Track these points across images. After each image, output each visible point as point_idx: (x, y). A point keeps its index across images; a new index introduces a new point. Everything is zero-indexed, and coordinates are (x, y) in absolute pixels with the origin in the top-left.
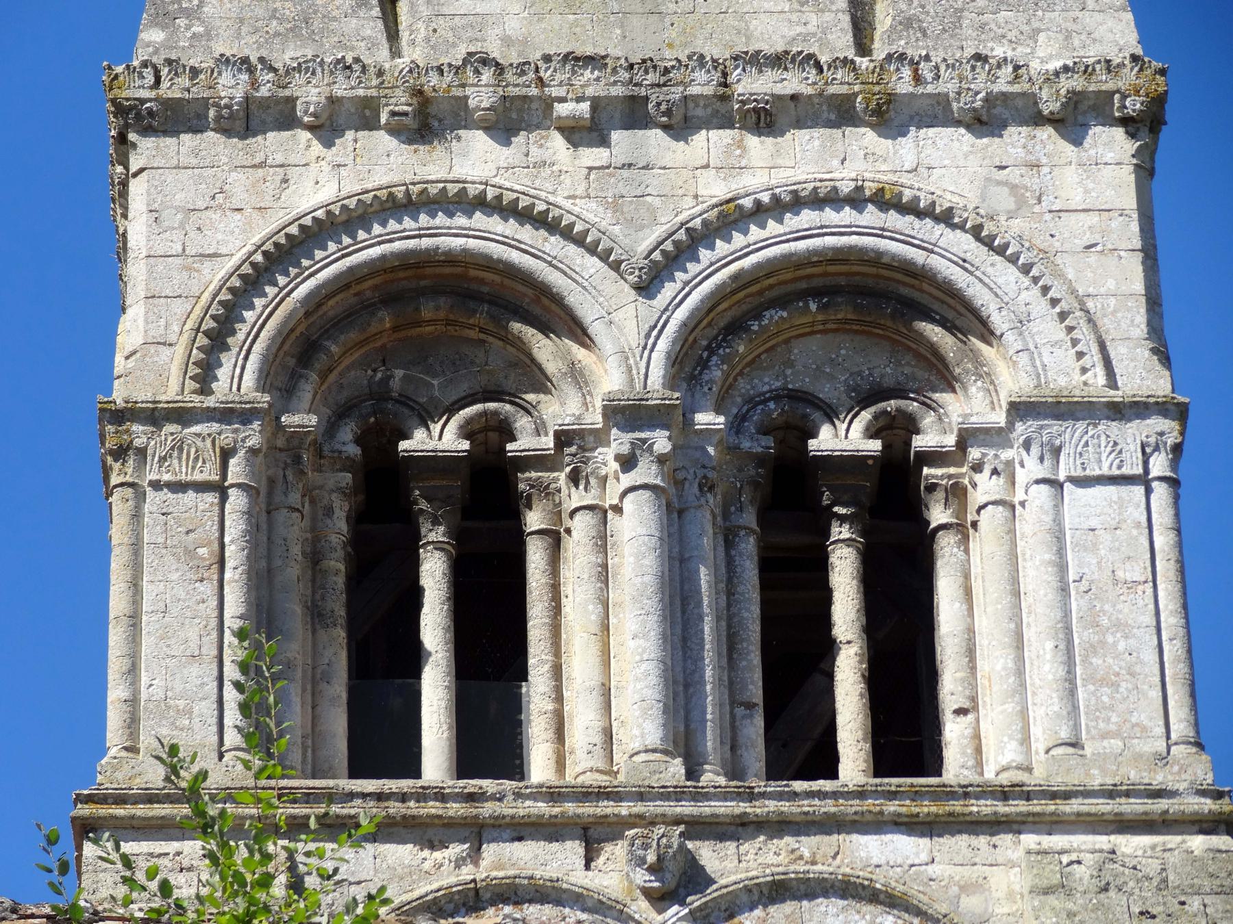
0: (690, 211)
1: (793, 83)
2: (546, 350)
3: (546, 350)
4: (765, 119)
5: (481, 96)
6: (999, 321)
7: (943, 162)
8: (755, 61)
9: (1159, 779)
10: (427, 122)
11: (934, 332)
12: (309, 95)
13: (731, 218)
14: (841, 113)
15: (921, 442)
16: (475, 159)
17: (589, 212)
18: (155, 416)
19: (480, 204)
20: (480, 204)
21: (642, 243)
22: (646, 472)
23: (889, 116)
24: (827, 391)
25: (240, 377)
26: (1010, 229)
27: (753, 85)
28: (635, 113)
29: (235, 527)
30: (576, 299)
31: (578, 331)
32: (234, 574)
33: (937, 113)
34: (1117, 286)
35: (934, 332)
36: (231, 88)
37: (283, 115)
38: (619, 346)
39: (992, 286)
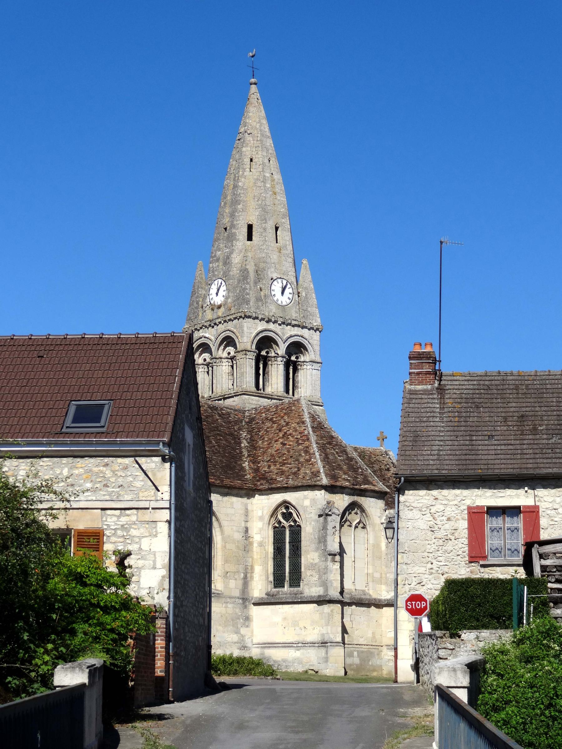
0: (288, 335)
1: (296, 323)
2: (274, 346)
3: (274, 346)
4: (294, 326)
5: (273, 320)
6: (309, 351)
7: (305, 332)
8: (294, 320)
9: (319, 401)
10: (268, 321)
11: (302, 349)
12: (260, 317)
13: (291, 336)
14: (298, 326)
15: (299, 360)
16: (271, 326)
17: (280, 333)
18: (248, 351)
19: (272, 331)
20: (272, 331)
21: (285, 338)
22: (283, 363)
23: (303, 327)
24: (293, 353)
25: (254, 347)
26: (310, 341)
27: (294, 322)
28: (283, 323)
29: (254, 364)
30: (278, 343)
31: (278, 345)
32: (254, 368)
33: (306, 327)
34: (317, 348)
35: (302, 349)
36: (254, 315)
37: (256, 318)
38: (282, 350)
39: (309, 347)
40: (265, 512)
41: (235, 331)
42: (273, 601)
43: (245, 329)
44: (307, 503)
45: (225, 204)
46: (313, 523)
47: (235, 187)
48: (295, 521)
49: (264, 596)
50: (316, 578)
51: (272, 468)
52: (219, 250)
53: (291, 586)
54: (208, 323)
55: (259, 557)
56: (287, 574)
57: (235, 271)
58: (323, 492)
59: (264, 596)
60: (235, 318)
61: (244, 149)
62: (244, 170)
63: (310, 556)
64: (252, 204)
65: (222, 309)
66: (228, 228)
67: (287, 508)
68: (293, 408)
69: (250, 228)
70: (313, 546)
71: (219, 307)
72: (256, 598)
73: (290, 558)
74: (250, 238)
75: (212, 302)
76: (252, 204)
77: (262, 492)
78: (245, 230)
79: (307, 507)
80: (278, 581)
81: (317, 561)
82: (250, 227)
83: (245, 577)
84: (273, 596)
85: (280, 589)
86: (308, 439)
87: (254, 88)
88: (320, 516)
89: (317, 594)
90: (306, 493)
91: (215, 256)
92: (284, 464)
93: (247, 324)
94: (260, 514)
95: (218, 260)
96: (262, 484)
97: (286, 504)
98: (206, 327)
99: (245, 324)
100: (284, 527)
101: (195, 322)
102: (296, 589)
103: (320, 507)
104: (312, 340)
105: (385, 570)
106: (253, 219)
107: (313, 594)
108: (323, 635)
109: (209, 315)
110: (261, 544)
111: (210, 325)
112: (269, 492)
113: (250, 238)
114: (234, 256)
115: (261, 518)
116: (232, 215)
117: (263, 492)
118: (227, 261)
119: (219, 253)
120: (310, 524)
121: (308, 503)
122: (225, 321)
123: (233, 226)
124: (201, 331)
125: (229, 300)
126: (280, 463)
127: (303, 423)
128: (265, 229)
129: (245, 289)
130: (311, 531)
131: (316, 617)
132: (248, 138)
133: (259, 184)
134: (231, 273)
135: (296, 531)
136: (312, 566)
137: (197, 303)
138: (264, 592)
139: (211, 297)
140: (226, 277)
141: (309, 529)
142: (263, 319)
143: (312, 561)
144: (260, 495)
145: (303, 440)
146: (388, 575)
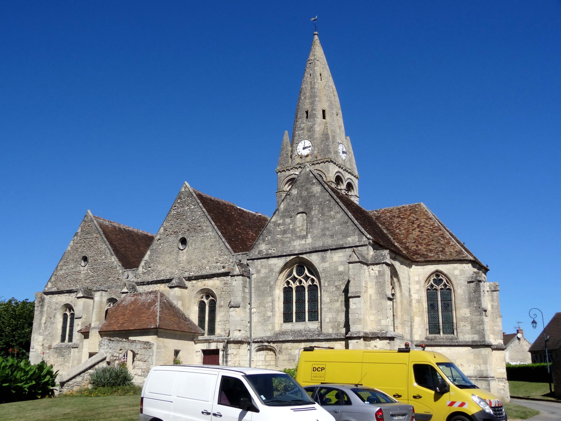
2: (340, 183)
3: (340, 183)
27: (349, 171)
40: (421, 278)
41: (322, 170)
42: (432, 343)
43: (330, 169)
44: (457, 272)
45: (305, 98)
46: (463, 287)
47: (312, 88)
48: (445, 285)
49: (424, 339)
50: (469, 327)
51: (420, 247)
52: (303, 123)
53: (444, 333)
54: (299, 166)
55: (418, 310)
56: (441, 324)
57: (317, 135)
58: (470, 265)
59: (424, 339)
60: (322, 162)
61: (316, 68)
62: (317, 79)
63: (462, 311)
64: (324, 99)
65: (310, 157)
66: (309, 111)
67: (438, 276)
68: (417, 209)
69: (324, 111)
70: (465, 304)
71: (307, 156)
72: (417, 341)
73: (442, 312)
74: (324, 117)
75: (299, 154)
76: (324, 99)
77: (418, 263)
78: (321, 113)
79: (457, 275)
80: (433, 328)
81: (468, 315)
82: (324, 111)
83: (411, 326)
84: (431, 340)
85: (436, 335)
86: (440, 229)
87: (316, 37)
88: (469, 282)
89: (471, 340)
90: (456, 265)
91: (300, 127)
92: (429, 245)
93: (331, 165)
94: (417, 279)
95: (303, 129)
96: (417, 258)
97: (437, 273)
98: (296, 168)
99: (330, 166)
100: (436, 289)
101: (287, 165)
102: (450, 336)
103: (468, 275)
104: (355, 182)
105: (492, 324)
106: (325, 107)
107: (467, 340)
108: (481, 371)
109: (298, 160)
110: (419, 301)
111: (300, 167)
112: (424, 263)
113: (324, 117)
114: (316, 126)
115: (418, 282)
116: (312, 103)
117: (419, 264)
118: (311, 129)
119: (303, 125)
120: (461, 288)
121: (459, 273)
122: (313, 164)
123: (313, 109)
124: (291, 171)
125: (315, 152)
126: (425, 244)
127: (430, 219)
128: (333, 113)
129: (328, 145)
130: (462, 293)
131: (471, 357)
132: (317, 63)
133: (327, 88)
134: (315, 136)
135: (447, 293)
136: (465, 319)
137: (287, 154)
138: (424, 336)
139: (298, 151)
140: (310, 138)
141: (460, 291)
142: (337, 165)
143: (464, 315)
144: (416, 265)
145: (436, 230)
146: (495, 328)
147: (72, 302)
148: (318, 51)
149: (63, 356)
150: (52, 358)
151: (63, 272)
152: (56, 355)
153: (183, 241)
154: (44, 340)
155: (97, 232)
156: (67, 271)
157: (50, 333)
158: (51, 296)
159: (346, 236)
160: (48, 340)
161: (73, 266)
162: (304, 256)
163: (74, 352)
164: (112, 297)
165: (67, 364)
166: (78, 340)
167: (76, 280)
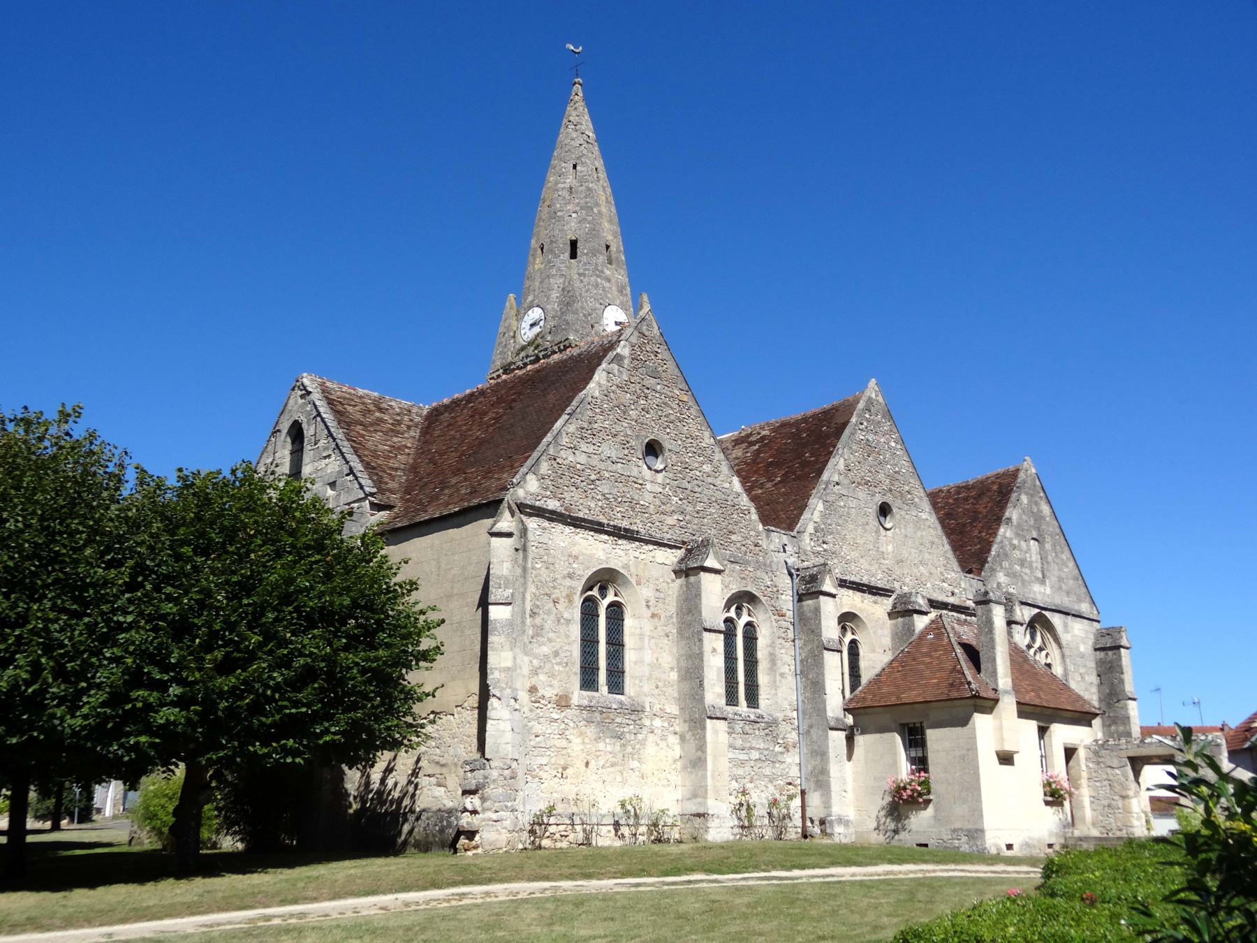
147: (626, 566)
148: (579, 126)
149: (619, 737)
150: (576, 741)
151: (582, 458)
152: (591, 731)
153: (884, 510)
154: (535, 672)
155: (683, 386)
156: (595, 461)
157: (556, 654)
158: (546, 524)
159: (1080, 601)
160: (552, 675)
161: (614, 455)
162: (1047, 614)
163: (716, 732)
164: (748, 589)
165: (635, 764)
166: (719, 695)
167: (633, 504)
